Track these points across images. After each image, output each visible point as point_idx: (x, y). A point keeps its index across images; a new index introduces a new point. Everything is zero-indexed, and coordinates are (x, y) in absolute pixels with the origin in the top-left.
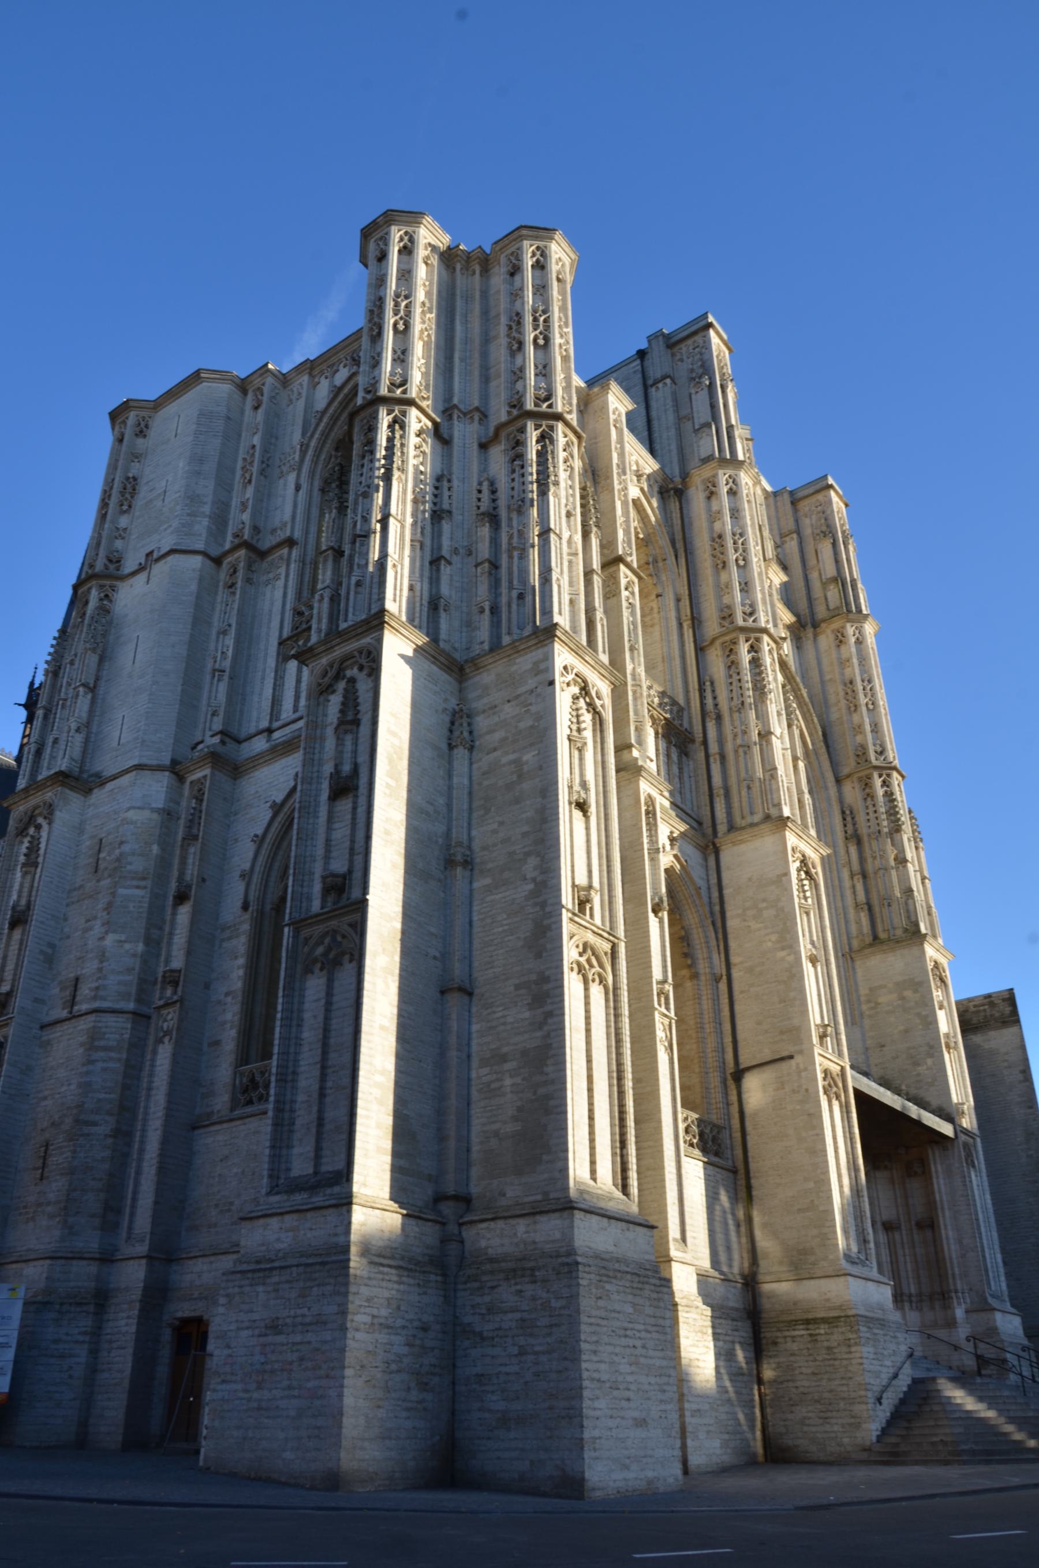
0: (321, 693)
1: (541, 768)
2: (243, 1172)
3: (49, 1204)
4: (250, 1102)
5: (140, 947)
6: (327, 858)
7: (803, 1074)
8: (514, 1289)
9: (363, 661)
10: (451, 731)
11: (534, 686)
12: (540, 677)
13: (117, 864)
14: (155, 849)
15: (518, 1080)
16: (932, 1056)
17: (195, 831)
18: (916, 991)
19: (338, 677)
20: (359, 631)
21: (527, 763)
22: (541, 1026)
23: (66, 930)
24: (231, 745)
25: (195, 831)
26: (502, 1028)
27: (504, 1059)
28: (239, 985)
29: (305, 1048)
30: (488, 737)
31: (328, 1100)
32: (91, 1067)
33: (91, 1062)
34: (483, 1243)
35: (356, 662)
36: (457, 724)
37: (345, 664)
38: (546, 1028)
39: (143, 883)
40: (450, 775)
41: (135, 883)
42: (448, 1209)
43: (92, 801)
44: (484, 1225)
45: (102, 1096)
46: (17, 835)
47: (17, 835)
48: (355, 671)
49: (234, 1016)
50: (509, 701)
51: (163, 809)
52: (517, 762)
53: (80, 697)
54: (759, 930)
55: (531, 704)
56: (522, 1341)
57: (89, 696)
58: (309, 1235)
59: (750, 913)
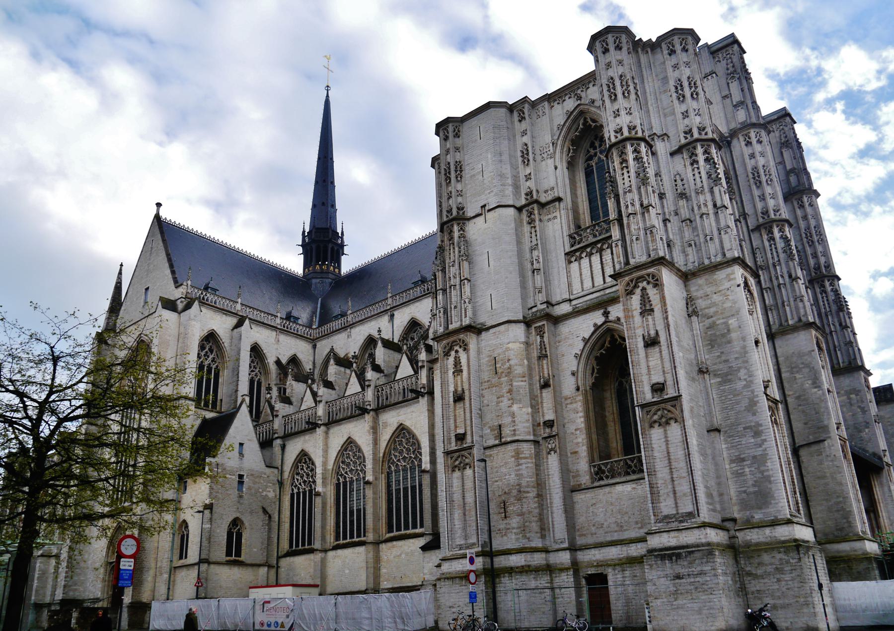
0: (628, 294)
1: (740, 327)
2: (606, 510)
3: (513, 528)
4: (601, 479)
5: (530, 410)
6: (649, 373)
7: (832, 448)
8: (770, 556)
9: (651, 280)
10: (687, 308)
11: (729, 286)
12: (732, 282)
14: (526, 362)
15: (753, 469)
16: (868, 427)
17: (544, 352)
18: (857, 395)
19: (636, 286)
21: (731, 324)
22: (760, 446)
23: (485, 402)
24: (551, 308)
25: (544, 352)
26: (740, 446)
27: (743, 460)
28: (583, 425)
29: (658, 460)
30: (706, 310)
31: (676, 483)
32: (520, 467)
33: (519, 465)
34: (749, 538)
35: (646, 280)
38: (764, 446)
39: (524, 379)
40: (692, 330)
41: (520, 379)
42: (728, 525)
44: (748, 530)
45: (528, 479)
46: (445, 355)
47: (445, 355)
48: (645, 283)
49: (583, 440)
52: (726, 324)
54: (801, 378)
56: (778, 576)
58: (685, 539)
59: (794, 370)
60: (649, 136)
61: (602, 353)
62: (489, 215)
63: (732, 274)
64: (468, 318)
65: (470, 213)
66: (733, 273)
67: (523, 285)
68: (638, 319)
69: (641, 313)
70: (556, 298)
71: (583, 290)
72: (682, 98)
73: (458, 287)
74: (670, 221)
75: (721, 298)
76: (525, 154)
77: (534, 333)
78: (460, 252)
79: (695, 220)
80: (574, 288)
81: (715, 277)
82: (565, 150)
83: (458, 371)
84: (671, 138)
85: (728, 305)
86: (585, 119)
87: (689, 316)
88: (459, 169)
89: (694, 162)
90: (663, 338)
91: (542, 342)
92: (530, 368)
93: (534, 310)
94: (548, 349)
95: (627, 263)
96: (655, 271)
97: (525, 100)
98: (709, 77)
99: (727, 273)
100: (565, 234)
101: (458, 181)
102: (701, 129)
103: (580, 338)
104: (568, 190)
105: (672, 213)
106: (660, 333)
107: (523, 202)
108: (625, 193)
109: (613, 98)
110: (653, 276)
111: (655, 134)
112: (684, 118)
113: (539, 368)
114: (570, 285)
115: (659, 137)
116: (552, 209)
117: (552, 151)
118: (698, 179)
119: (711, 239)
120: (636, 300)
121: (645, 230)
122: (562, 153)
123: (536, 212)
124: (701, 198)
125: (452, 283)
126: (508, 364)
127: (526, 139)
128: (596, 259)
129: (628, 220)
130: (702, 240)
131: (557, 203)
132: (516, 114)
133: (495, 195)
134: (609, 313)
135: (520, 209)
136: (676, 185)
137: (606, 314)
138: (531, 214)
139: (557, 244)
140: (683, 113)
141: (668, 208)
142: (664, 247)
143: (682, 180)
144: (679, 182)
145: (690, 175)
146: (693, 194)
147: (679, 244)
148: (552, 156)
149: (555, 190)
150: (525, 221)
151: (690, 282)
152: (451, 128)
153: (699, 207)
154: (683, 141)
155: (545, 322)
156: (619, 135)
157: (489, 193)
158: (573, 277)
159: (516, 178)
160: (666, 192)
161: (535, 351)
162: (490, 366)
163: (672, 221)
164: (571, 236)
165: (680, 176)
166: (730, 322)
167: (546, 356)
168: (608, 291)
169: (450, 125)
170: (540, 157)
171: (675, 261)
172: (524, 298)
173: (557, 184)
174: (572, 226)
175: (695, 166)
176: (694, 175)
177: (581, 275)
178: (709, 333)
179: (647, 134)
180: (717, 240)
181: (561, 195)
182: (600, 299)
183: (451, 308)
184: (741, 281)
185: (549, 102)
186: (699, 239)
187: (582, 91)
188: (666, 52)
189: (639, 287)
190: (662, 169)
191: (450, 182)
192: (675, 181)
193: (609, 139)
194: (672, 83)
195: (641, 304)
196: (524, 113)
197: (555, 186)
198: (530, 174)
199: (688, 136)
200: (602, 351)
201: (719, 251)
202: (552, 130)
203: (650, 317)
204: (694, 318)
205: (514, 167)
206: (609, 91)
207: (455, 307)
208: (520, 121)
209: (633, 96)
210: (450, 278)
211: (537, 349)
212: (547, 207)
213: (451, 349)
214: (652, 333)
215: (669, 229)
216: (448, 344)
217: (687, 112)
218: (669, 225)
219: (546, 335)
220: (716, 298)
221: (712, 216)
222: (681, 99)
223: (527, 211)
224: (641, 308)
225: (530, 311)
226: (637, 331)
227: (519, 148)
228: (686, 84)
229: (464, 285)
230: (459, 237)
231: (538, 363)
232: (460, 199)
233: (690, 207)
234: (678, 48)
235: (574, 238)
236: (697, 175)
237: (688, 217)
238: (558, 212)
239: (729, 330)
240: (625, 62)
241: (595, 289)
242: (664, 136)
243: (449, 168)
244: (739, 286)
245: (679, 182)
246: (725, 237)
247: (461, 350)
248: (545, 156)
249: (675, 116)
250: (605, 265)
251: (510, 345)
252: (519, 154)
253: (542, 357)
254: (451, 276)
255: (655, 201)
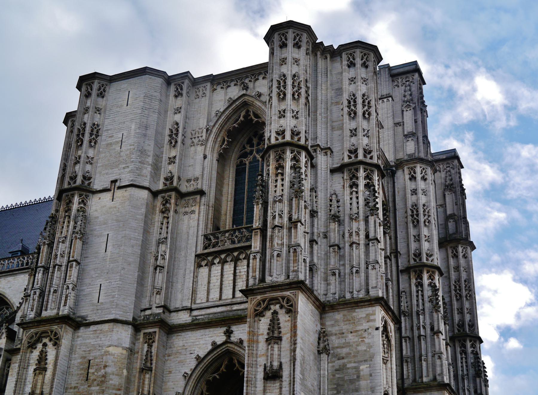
0: (256, 315)
1: (371, 375)
9: (285, 304)
10: (319, 343)
11: (367, 328)
12: (370, 324)
13: (103, 379)
14: (125, 371)
17: (149, 364)
19: (267, 308)
20: (283, 287)
21: (363, 370)
24: (167, 314)
25: (149, 364)
30: (339, 350)
35: (279, 303)
36: (322, 339)
37: (271, 302)
40: (319, 369)
43: (80, 334)
47: (29, 347)
48: (278, 306)
50: (351, 332)
51: (129, 348)
52: (357, 369)
53: (74, 268)
55: (364, 338)
57: (78, 267)
60: (311, 147)
61: (215, 377)
62: (119, 193)
63: (372, 315)
64: (67, 307)
65: (97, 185)
66: (374, 314)
67: (141, 281)
68: (262, 346)
69: (267, 340)
70: (176, 304)
71: (207, 301)
72: (353, 114)
73: (63, 268)
74: (317, 243)
75: (356, 339)
76: (174, 134)
77: (141, 340)
78: (75, 228)
79: (344, 248)
80: (199, 296)
81: (354, 314)
82: (219, 139)
83: (41, 368)
84: (335, 154)
85: (362, 348)
86: (248, 111)
87: (319, 353)
88: (95, 133)
89: (354, 185)
90: (286, 373)
91: (149, 352)
92: (128, 380)
93: (148, 312)
94: (154, 362)
95: (262, 280)
96: (291, 295)
97: (186, 75)
98: (385, 100)
99: (368, 312)
100: (200, 233)
101: (91, 146)
102: (367, 152)
103: (194, 356)
104: (214, 185)
105: (321, 235)
106: (283, 367)
107: (161, 186)
108: (275, 202)
109: (282, 96)
110: (288, 301)
111: (318, 145)
112: (352, 136)
113: (139, 382)
114: (194, 292)
115: (322, 149)
116: (191, 201)
117: (204, 137)
118: (355, 205)
119: (357, 272)
120: (264, 323)
121: (289, 247)
122: (215, 142)
123: (173, 201)
124: (355, 225)
125: (58, 262)
126: (103, 371)
127: (178, 118)
128: (229, 268)
129: (273, 232)
130: (347, 271)
131: (198, 197)
132: (173, 88)
133: (130, 172)
134: (232, 332)
135: (155, 194)
136: (331, 205)
137: (229, 333)
138: (167, 202)
139: (190, 242)
140: (351, 131)
141: (318, 228)
142: (306, 270)
143: (338, 201)
144: (334, 203)
145: (347, 198)
146: (347, 219)
147: (323, 270)
148: (204, 143)
149: (200, 181)
150: (158, 209)
151: (327, 315)
152: (96, 85)
153: (351, 235)
154: (346, 160)
155: (157, 330)
156: (280, 138)
157: (124, 168)
158: (199, 283)
159: (158, 158)
160: (319, 211)
161: (139, 361)
162: (82, 369)
163: (319, 243)
164: (206, 237)
165: (337, 196)
166: (361, 367)
167: (150, 369)
168: (235, 307)
169: (96, 82)
170: (190, 141)
171: (315, 288)
172: (139, 296)
173: (203, 175)
174: (210, 226)
175: (354, 189)
176: (351, 199)
177: (209, 283)
178: (337, 376)
179: (310, 143)
180: (363, 275)
181: (205, 188)
182: (225, 314)
183: (50, 291)
184: (380, 324)
185: (212, 84)
186: (345, 269)
187: (250, 81)
188: (345, 63)
189: (270, 309)
190: (319, 185)
191: (81, 145)
192: (331, 200)
193: (269, 139)
194: (346, 96)
195: (269, 329)
196: (182, 89)
197: (200, 177)
198: (175, 157)
199: (353, 156)
200: (215, 375)
201: (363, 287)
202: (209, 114)
203: (276, 346)
204: (324, 356)
205: (158, 145)
206: (279, 88)
207: (55, 292)
208: (176, 96)
209: (303, 100)
210: (56, 255)
211: (141, 360)
212: (187, 198)
213: (39, 340)
214: (276, 364)
215: (315, 252)
216: (36, 334)
217: (355, 130)
218: (315, 247)
219: (155, 345)
220: (351, 338)
221: (362, 247)
222: (352, 115)
223: (163, 197)
224: (268, 334)
225: (143, 314)
226: (259, 359)
227: (169, 126)
228: (359, 101)
229: (71, 267)
230: (78, 211)
231: (140, 376)
232: (88, 167)
233: (341, 233)
234: (358, 62)
235: (210, 240)
236: (354, 199)
237: (337, 242)
238: (197, 207)
239: (358, 377)
240: (302, 62)
241: (221, 302)
242: (328, 150)
243: (84, 129)
244: (377, 329)
245: (334, 203)
246: (372, 273)
247: (50, 345)
248: (196, 141)
249: (343, 132)
250: (238, 277)
251: (111, 349)
252: (167, 132)
253: (146, 369)
254: (59, 253)
255: (305, 217)
